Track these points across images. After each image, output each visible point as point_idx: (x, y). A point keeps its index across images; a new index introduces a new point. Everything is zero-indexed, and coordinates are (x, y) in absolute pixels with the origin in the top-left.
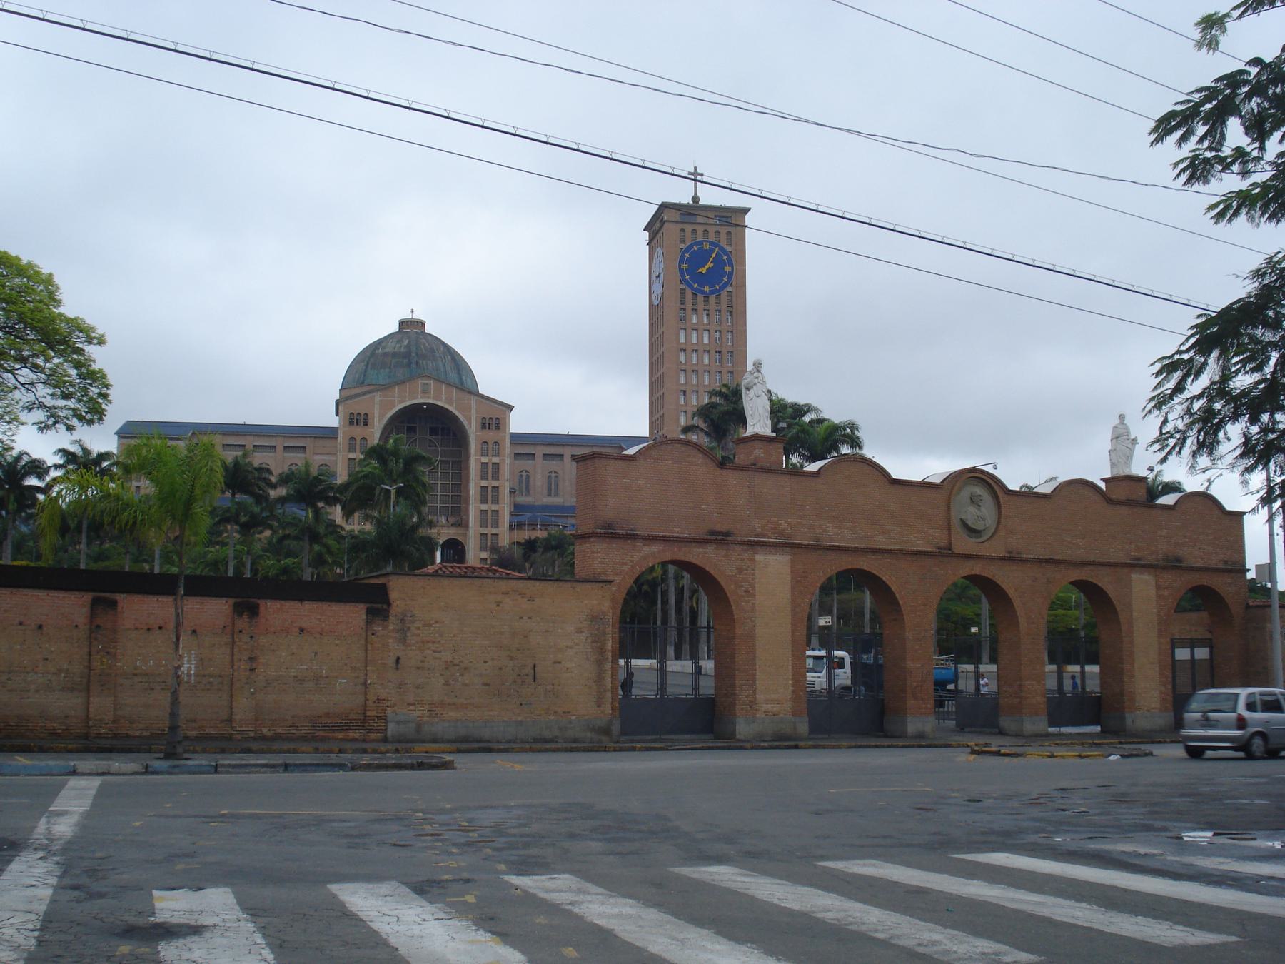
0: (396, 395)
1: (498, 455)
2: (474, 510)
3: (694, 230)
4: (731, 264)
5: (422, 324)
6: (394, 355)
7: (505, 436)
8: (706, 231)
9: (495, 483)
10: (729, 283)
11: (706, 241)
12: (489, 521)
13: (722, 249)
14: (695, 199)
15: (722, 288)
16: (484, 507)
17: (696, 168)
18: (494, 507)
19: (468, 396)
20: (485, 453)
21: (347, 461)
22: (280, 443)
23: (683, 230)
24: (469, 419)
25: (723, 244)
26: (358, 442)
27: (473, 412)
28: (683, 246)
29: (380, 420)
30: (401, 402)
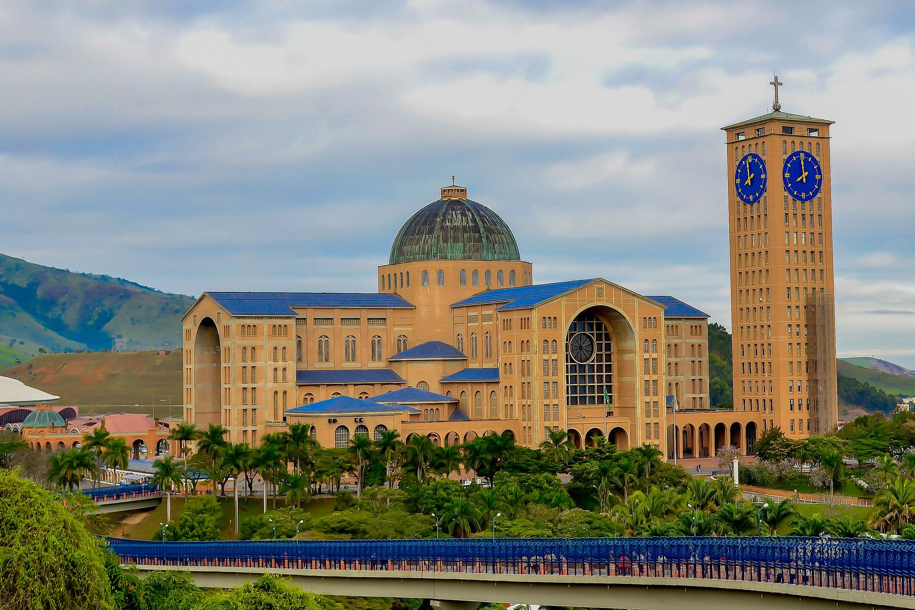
0: (578, 299)
4: (820, 174)
6: (465, 229)
9: (655, 377)
10: (817, 191)
13: (813, 159)
14: (777, 109)
15: (815, 194)
16: (647, 399)
17: (776, 78)
19: (632, 298)
20: (646, 351)
22: (364, 314)
25: (814, 154)
27: (637, 312)
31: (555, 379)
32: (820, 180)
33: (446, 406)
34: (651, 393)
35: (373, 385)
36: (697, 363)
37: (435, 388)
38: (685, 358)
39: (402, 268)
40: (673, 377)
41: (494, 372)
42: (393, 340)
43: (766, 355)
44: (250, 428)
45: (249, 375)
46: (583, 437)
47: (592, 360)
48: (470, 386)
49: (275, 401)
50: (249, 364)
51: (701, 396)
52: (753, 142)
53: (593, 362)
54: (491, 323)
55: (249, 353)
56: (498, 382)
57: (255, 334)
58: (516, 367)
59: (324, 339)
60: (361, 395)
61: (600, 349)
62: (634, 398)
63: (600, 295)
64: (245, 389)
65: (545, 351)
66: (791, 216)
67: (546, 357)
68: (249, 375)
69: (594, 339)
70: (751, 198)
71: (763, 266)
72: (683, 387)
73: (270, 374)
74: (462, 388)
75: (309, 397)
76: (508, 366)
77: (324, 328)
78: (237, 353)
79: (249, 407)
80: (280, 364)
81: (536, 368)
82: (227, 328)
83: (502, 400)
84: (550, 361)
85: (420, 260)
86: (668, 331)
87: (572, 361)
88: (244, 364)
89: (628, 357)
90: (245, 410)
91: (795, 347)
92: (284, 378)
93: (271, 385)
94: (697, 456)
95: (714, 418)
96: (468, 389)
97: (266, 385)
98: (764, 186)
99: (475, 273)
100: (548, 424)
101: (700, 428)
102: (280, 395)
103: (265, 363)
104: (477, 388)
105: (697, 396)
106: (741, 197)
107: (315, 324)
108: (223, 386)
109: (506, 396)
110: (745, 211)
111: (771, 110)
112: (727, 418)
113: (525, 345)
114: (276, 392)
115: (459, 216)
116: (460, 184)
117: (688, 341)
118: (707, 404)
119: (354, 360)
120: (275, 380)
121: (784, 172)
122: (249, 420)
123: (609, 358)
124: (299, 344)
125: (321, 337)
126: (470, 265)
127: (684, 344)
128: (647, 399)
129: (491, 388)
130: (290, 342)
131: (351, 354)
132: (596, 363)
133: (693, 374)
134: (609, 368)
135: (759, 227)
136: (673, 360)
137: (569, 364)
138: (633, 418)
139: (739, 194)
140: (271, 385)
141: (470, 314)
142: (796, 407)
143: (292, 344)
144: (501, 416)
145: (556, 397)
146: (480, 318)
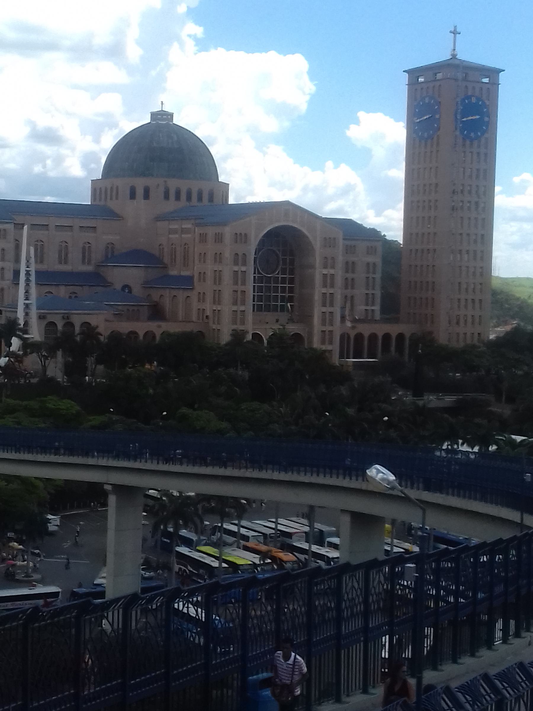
13: (483, 102)
14: (454, 56)
15: (483, 134)
31: (243, 288)
32: (488, 122)
35: (81, 286)
37: (137, 290)
51: (373, 308)
53: (278, 274)
59: (39, 243)
60: (71, 295)
70: (426, 135)
95: (381, 330)
100: (234, 327)
112: (394, 330)
118: (378, 316)
123: (292, 272)
128: (324, 309)
134: (292, 281)
137: (256, 275)
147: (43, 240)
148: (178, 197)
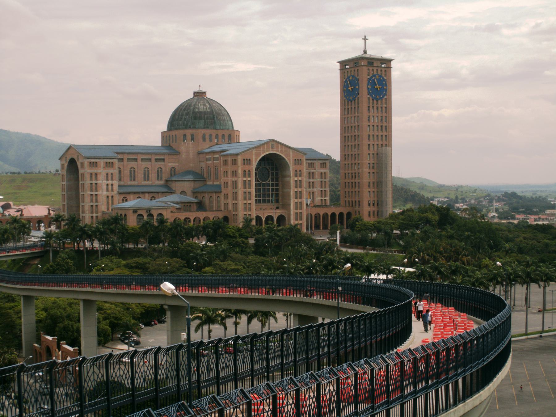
1: (301, 176)
2: (292, 202)
3: (373, 70)
4: (386, 86)
5: (205, 93)
7: (303, 168)
8: (377, 70)
9: (300, 190)
10: (385, 95)
11: (377, 75)
12: (298, 206)
13: (383, 78)
14: (365, 52)
15: (383, 96)
16: (296, 200)
17: (365, 36)
18: (300, 200)
21: (243, 182)
22: (154, 157)
23: (369, 69)
24: (289, 160)
25: (383, 75)
26: (247, 172)
27: (291, 157)
28: (369, 77)
29: (255, 162)
30: (263, 153)
31: (249, 190)
32: (386, 89)
33: (195, 204)
34: (298, 198)
36: (323, 183)
38: (317, 179)
39: (174, 133)
40: (311, 189)
41: (219, 186)
42: (168, 170)
43: (357, 178)
44: (94, 215)
45: (94, 188)
46: (264, 220)
47: (269, 181)
48: (207, 194)
49: (108, 201)
50: (94, 182)
51: (325, 198)
52: (353, 70)
53: (269, 181)
54: (218, 161)
55: (94, 177)
56: (221, 192)
57: (97, 166)
58: (230, 183)
59: (132, 169)
61: (273, 175)
62: (289, 200)
63: (272, 148)
64: (92, 195)
65: (245, 176)
66: (371, 108)
67: (245, 179)
68: (94, 188)
69: (270, 170)
70: (351, 98)
71: (356, 134)
72: (316, 194)
73: (105, 187)
74: (203, 195)
75: (125, 199)
76: (226, 184)
77: (133, 164)
78: (87, 176)
79: (94, 204)
80: (110, 182)
81: (240, 185)
82: (82, 164)
83: (223, 201)
84: (247, 181)
85: (183, 129)
86: (309, 165)
87: (258, 181)
88: (91, 182)
89: (287, 179)
90: (92, 206)
91: (372, 174)
92: (112, 190)
93: (105, 193)
94: (321, 228)
95: (329, 212)
96: (206, 195)
97: (103, 193)
98: (358, 92)
99: (211, 136)
101: (323, 215)
102: (110, 198)
103: (102, 182)
104: (210, 195)
105: (323, 198)
106: (346, 98)
107: (128, 162)
108: (81, 193)
109: (225, 199)
110: (348, 105)
111: (362, 53)
112: (337, 211)
113: (235, 173)
114: (108, 197)
115: (202, 106)
116: (203, 89)
117: (319, 171)
118: (328, 203)
119: (148, 180)
120: (108, 190)
121: (368, 85)
122: (94, 211)
123: (277, 180)
124: (120, 172)
125: (131, 168)
126: (208, 132)
127: (317, 173)
128: (296, 200)
129: (217, 195)
130: (115, 171)
131: (146, 177)
132: (270, 182)
133: (322, 187)
134: (277, 185)
135: (355, 113)
136: (311, 180)
137: (257, 183)
138: (289, 210)
139: (345, 96)
140: (105, 193)
141: (208, 157)
142: (371, 204)
143: (115, 171)
144: (222, 208)
145: (250, 199)
146: (212, 159)
147: (134, 167)
148: (211, 140)
